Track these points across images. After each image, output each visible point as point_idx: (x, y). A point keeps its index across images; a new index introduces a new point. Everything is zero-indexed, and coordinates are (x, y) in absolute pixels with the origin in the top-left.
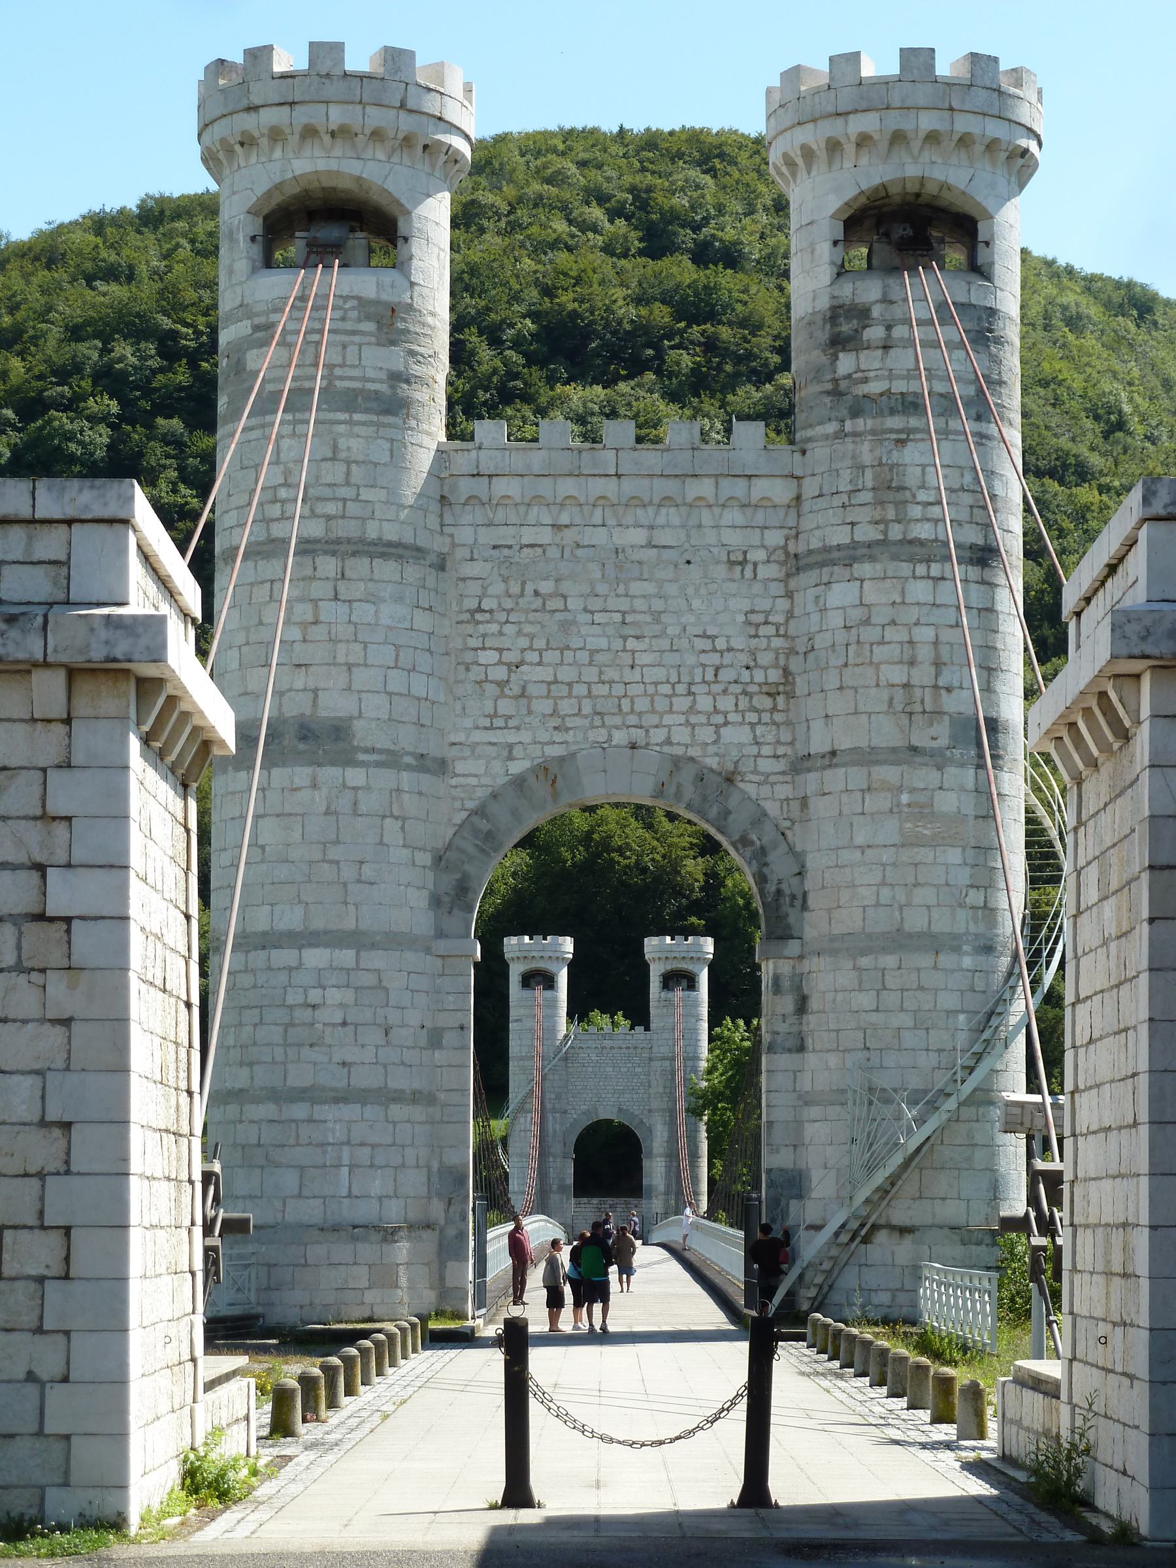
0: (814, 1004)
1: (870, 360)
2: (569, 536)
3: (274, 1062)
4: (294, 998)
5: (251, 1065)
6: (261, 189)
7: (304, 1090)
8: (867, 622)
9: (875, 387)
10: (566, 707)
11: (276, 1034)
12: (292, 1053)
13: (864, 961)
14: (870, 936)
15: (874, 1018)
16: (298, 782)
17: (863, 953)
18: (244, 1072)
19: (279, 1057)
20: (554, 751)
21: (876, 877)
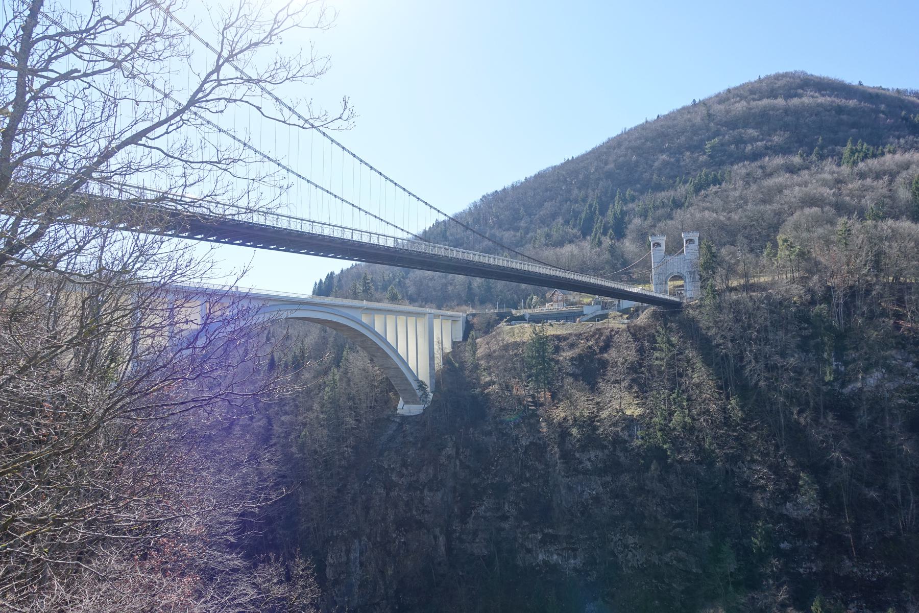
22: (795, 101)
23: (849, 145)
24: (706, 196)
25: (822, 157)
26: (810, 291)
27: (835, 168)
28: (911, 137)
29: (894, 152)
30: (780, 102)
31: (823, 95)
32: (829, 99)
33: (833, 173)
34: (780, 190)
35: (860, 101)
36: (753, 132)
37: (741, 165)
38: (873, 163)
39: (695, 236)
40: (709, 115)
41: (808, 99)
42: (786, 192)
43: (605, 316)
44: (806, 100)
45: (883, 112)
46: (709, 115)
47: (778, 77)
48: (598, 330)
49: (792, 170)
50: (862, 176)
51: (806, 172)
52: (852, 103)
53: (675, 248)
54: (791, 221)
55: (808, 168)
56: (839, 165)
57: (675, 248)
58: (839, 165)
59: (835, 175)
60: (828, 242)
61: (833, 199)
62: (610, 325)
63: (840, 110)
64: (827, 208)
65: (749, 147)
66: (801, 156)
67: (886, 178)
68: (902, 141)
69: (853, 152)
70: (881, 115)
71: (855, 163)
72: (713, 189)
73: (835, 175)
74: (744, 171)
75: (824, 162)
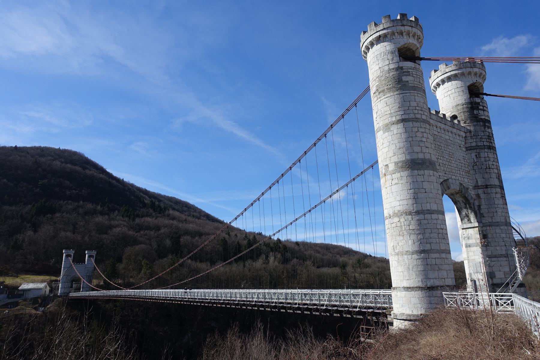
0: (489, 236)
1: (481, 112)
2: (440, 134)
3: (436, 243)
4: (439, 227)
5: (430, 243)
6: (402, 43)
7: (444, 250)
8: (490, 160)
9: (483, 117)
10: (445, 168)
11: (436, 235)
12: (440, 240)
13: (502, 227)
14: (502, 222)
15: (507, 239)
16: (431, 174)
17: (502, 226)
18: (428, 245)
19: (438, 242)
20: (446, 178)
21: (500, 210)
22: (88, 172)
24: (52, 218)
30: (78, 168)
36: (68, 183)
37: (66, 201)
39: (94, 253)
41: (90, 172)
42: (114, 229)
43: (17, 304)
44: (96, 174)
47: (75, 153)
48: (16, 316)
49: (102, 214)
51: (107, 216)
52: (114, 181)
53: (79, 259)
55: (108, 214)
57: (79, 259)
62: (27, 311)
65: (68, 193)
66: (101, 206)
71: (134, 220)
72: (58, 215)
74: (70, 207)
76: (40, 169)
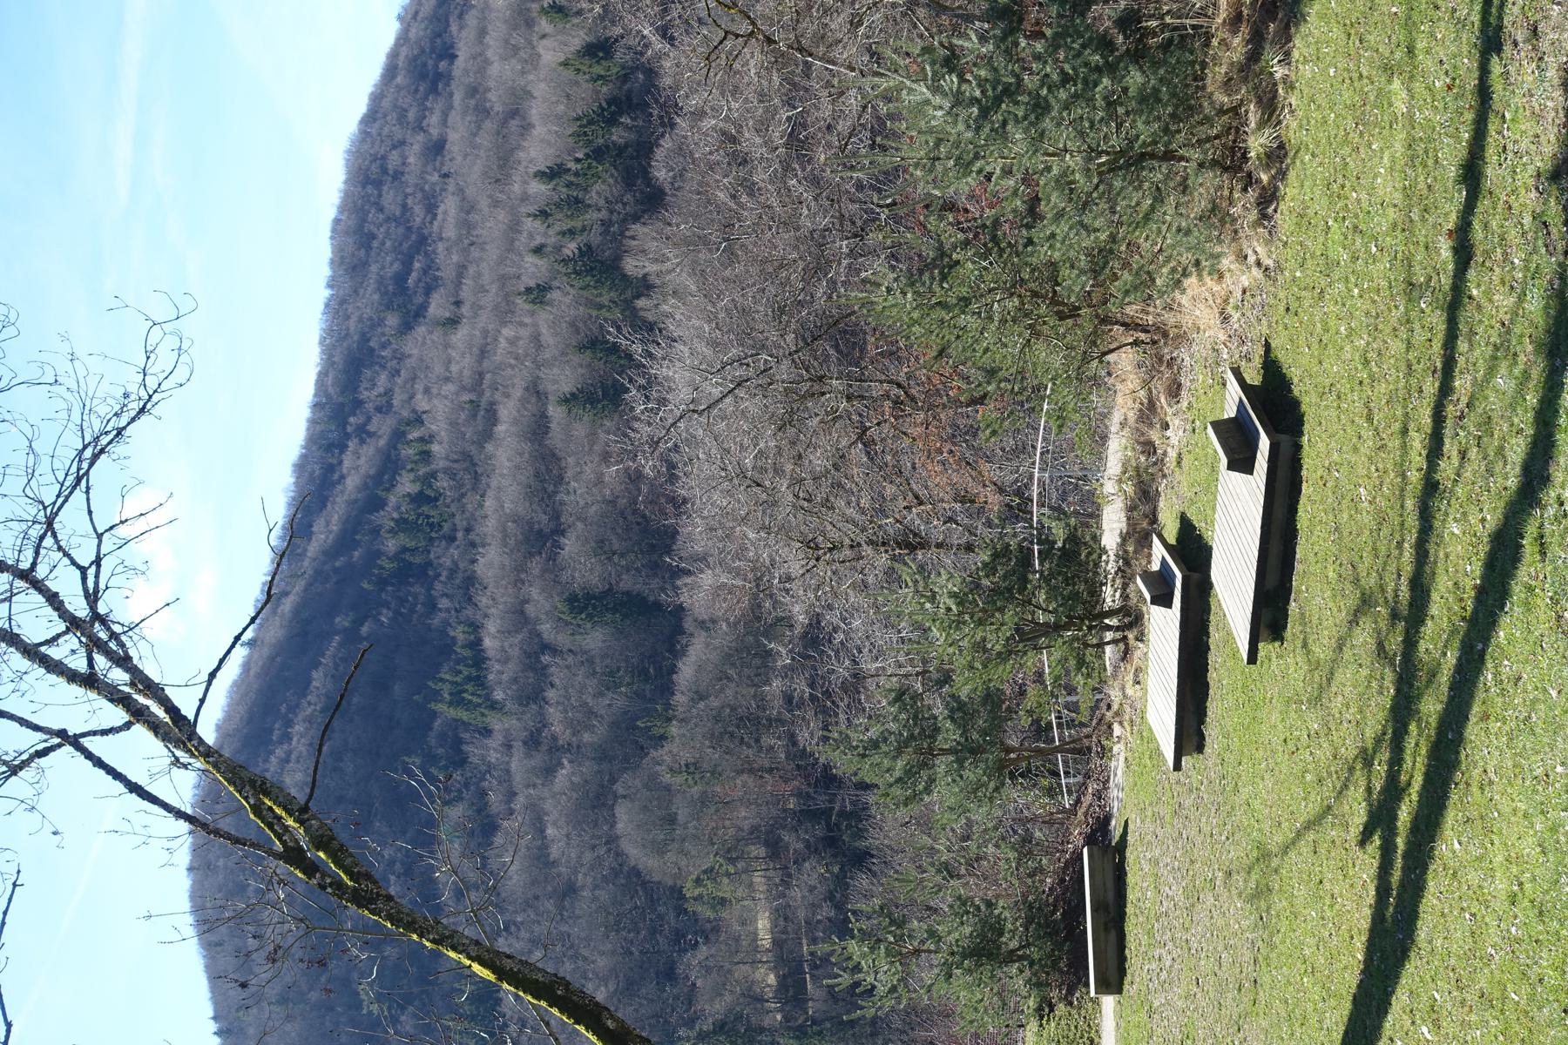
23: (441, 707)
25: (461, 761)
26: (812, 849)
27: (495, 742)
28: (438, 586)
29: (475, 627)
31: (287, 737)
32: (298, 728)
33: (508, 746)
34: (541, 858)
35: (317, 665)
38: (502, 677)
40: (283, 1000)
42: (555, 852)
45: (359, 622)
46: (283, 1000)
49: (485, 828)
50: (532, 696)
52: (318, 679)
54: (635, 853)
56: (487, 732)
58: (487, 732)
59: (518, 744)
60: (704, 800)
61: (588, 767)
63: (336, 707)
64: (619, 788)
67: (546, 659)
68: (444, 603)
69: (458, 700)
70: (365, 630)
73: (518, 744)
75: (474, 760)
76: (314, 996)
